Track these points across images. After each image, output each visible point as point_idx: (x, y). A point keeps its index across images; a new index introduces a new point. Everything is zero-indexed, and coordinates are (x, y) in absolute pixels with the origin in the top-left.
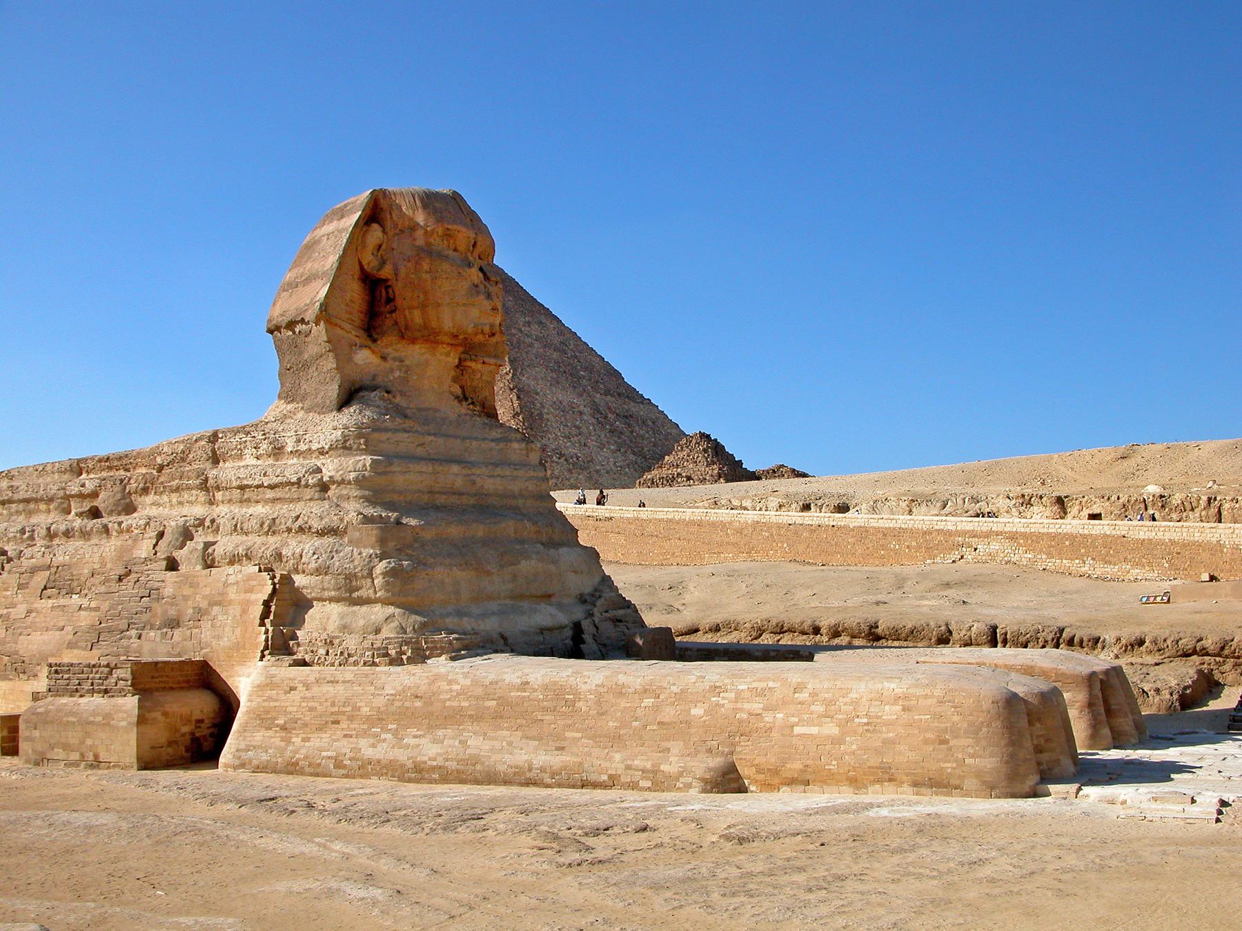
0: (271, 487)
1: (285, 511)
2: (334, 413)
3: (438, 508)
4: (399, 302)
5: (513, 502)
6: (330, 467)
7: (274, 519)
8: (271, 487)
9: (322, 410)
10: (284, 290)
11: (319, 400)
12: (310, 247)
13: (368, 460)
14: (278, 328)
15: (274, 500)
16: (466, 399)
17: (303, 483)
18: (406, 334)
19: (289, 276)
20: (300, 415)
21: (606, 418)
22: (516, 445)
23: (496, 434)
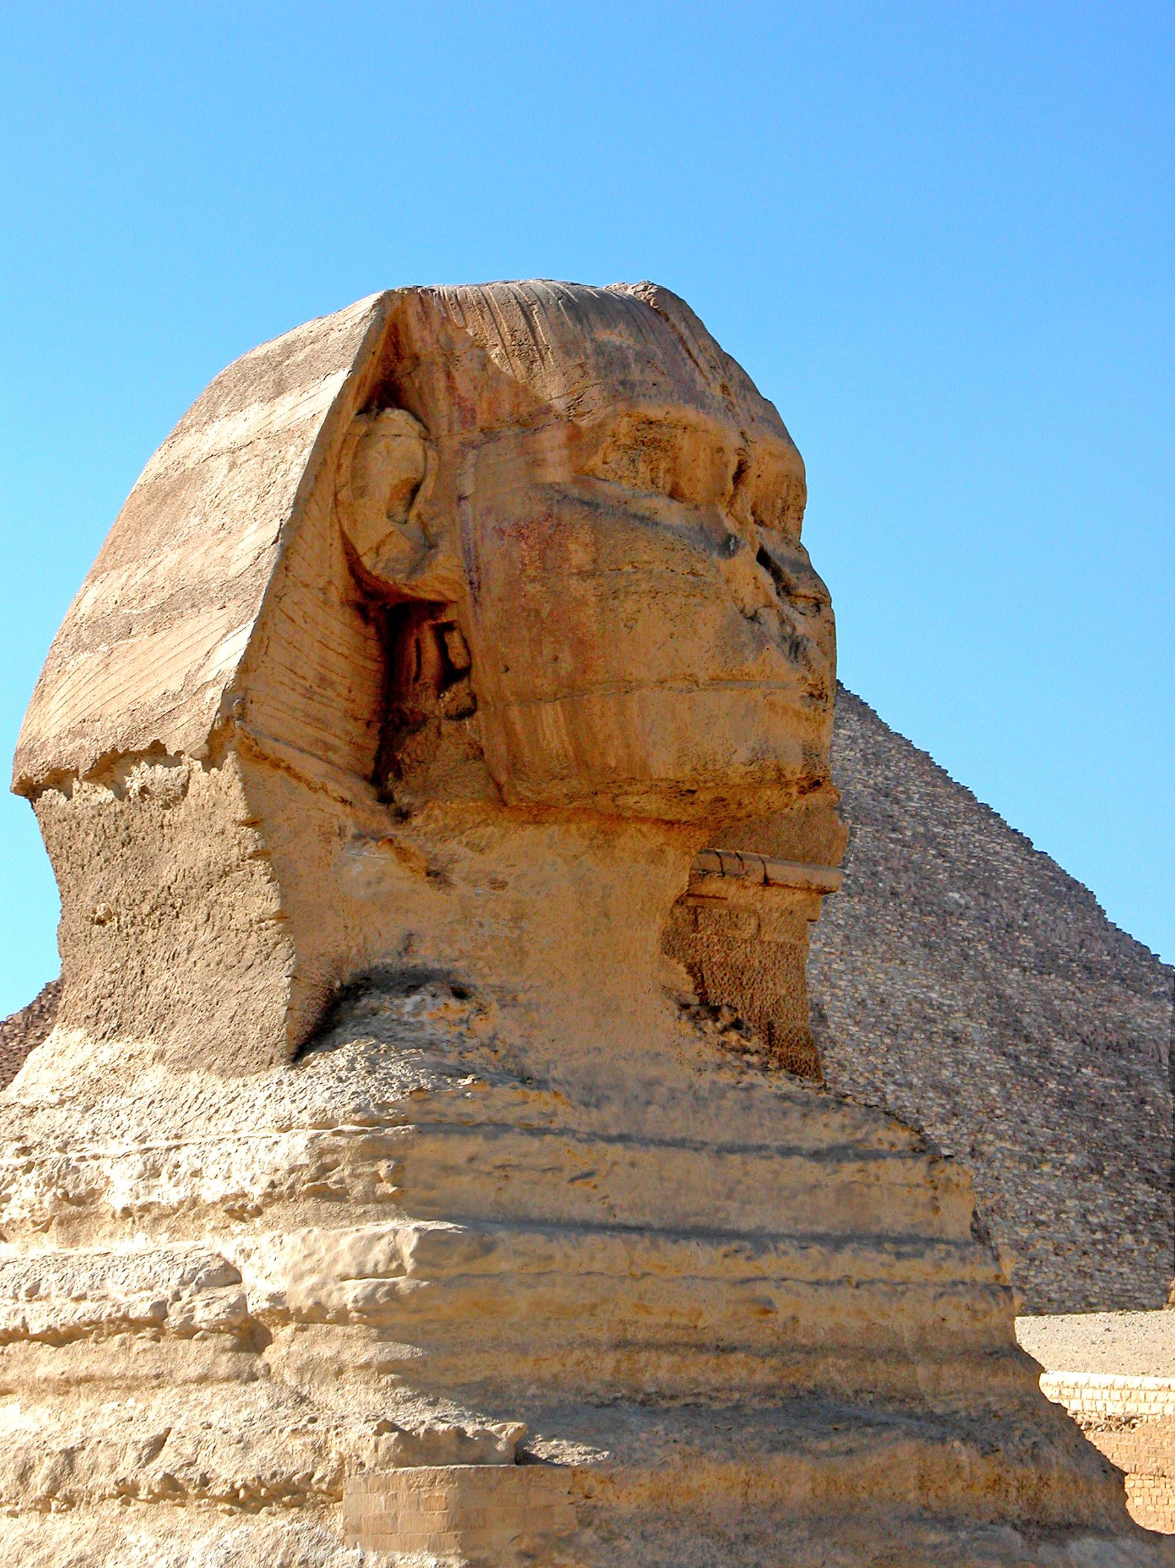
0: (58, 1338)
1: (109, 1425)
2: (278, 1071)
3: (648, 1404)
4: (484, 678)
5: (900, 1376)
6: (275, 1263)
7: (69, 1455)
8: (58, 1338)
9: (234, 1060)
11: (220, 1025)
12: (168, 493)
13: (406, 1234)
14: (60, 779)
15: (67, 1385)
16: (715, 1012)
17: (175, 1318)
18: (508, 794)
19: (93, 598)
20: (154, 1078)
21: (1044, 1052)
22: (894, 1170)
23: (826, 1130)
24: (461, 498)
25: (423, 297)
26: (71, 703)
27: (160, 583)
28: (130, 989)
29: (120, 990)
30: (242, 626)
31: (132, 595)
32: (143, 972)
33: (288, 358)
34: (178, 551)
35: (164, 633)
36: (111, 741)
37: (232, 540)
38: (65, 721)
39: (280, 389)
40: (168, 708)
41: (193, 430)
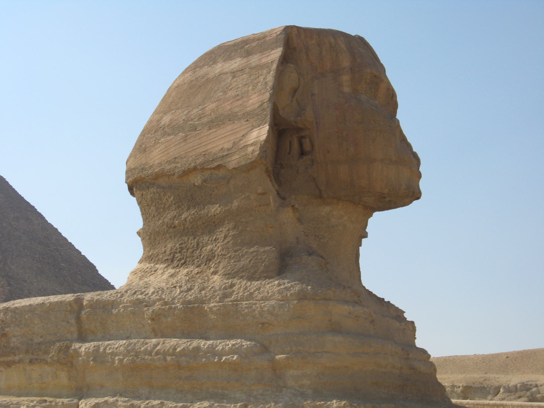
10: (165, 134)
24: (312, 95)
25: (298, 28)
26: (166, 153)
27: (207, 113)
28: (190, 250)
29: (185, 250)
30: (261, 127)
31: (192, 117)
32: (198, 245)
33: (247, 45)
34: (215, 104)
35: (216, 129)
36: (193, 165)
37: (245, 99)
38: (164, 158)
39: (249, 53)
40: (225, 154)
41: (206, 67)
